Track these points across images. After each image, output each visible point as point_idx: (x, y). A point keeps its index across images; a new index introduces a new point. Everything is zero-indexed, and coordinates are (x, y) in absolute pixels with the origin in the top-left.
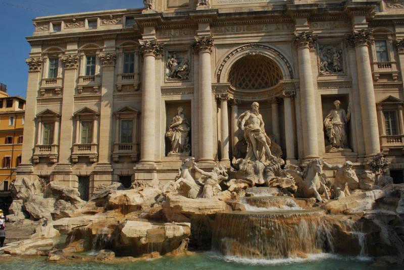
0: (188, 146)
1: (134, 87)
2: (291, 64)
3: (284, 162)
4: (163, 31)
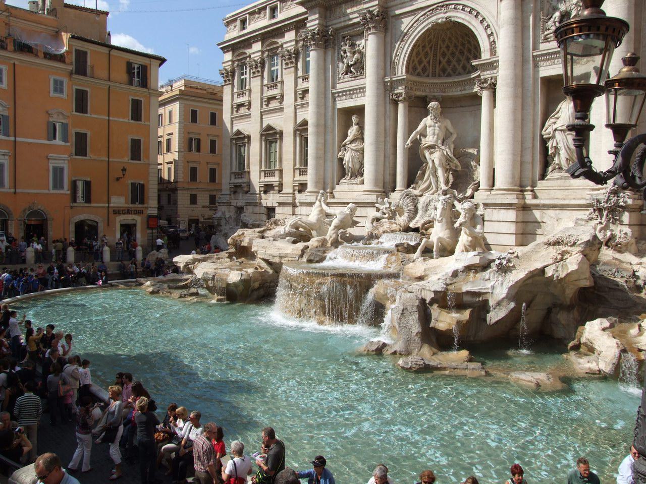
2: (493, 29)
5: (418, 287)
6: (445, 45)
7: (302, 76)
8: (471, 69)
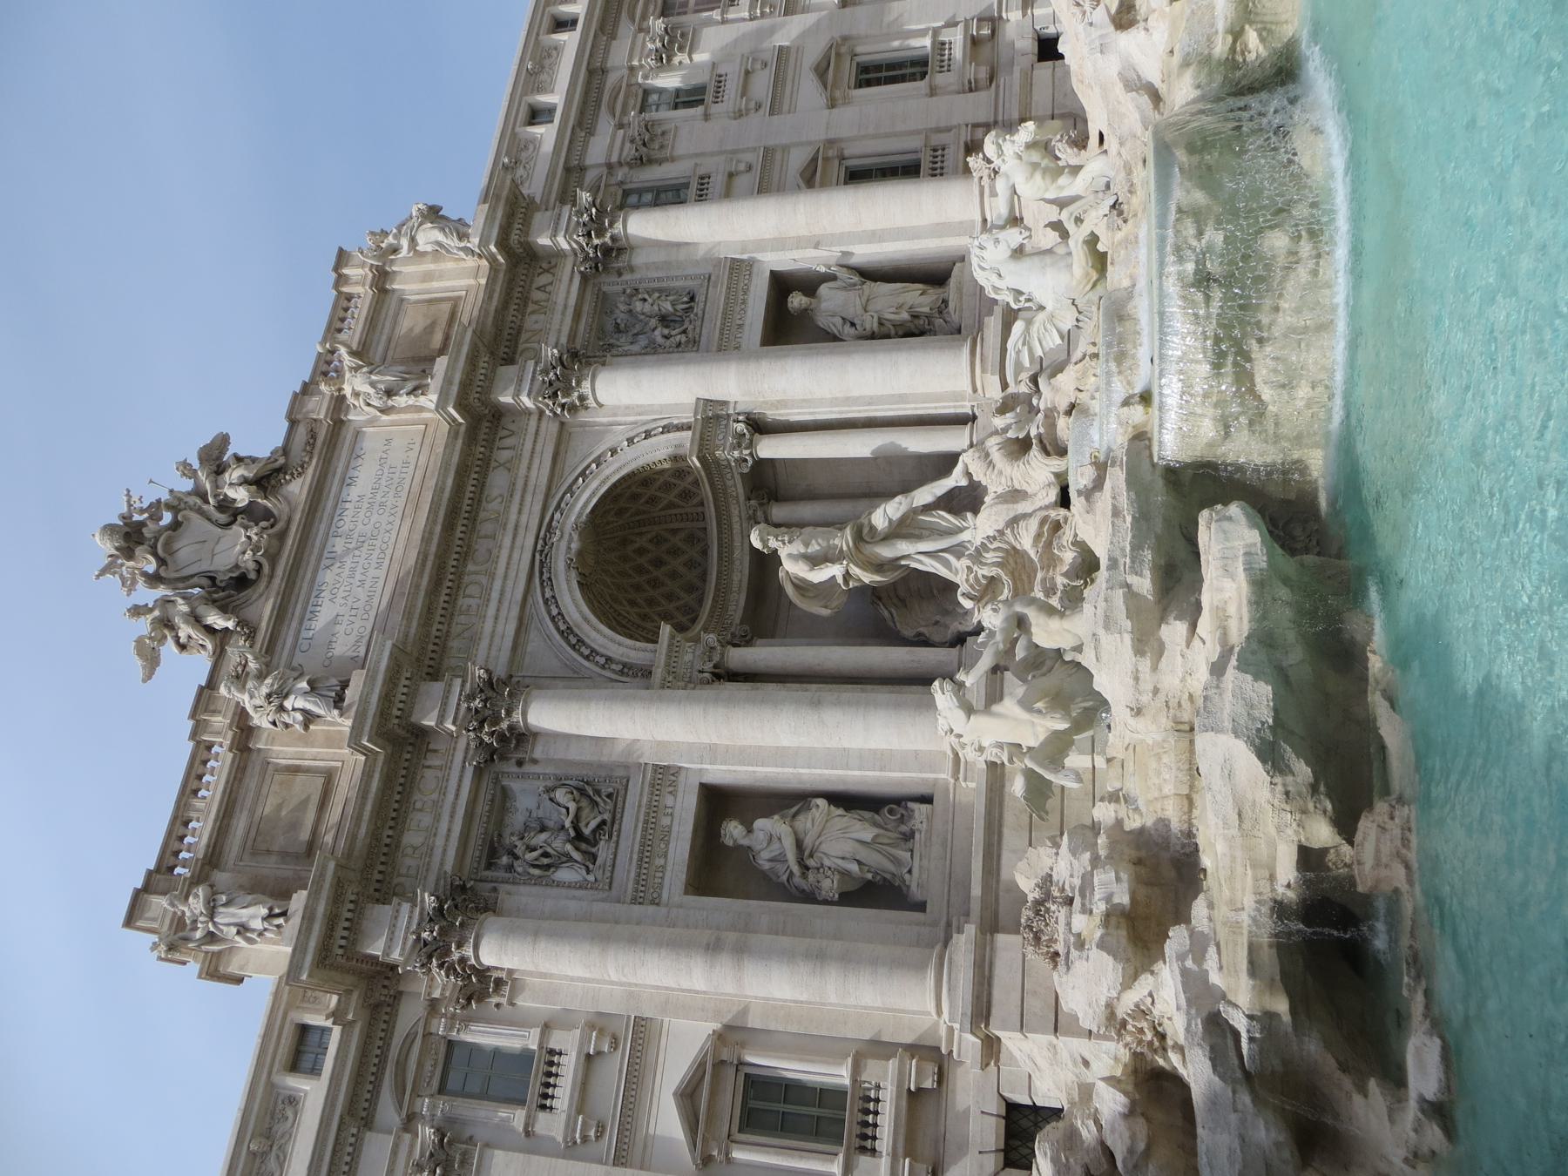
0: (891, 812)
1: (599, 1053)
4: (395, 881)
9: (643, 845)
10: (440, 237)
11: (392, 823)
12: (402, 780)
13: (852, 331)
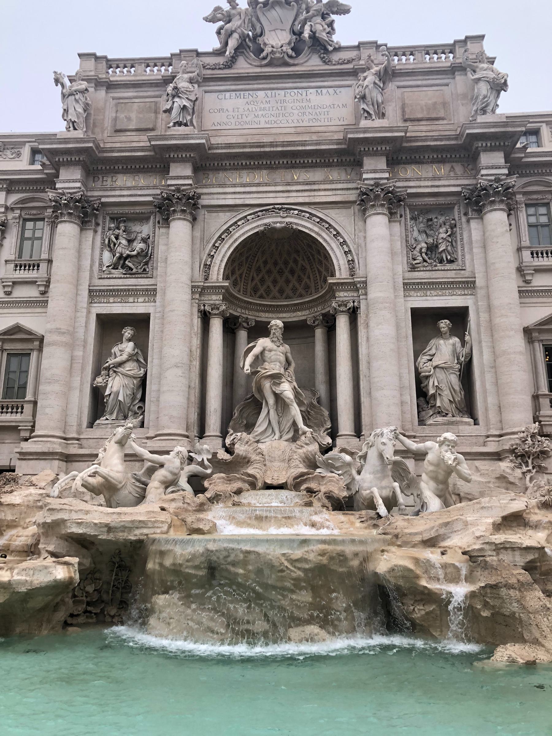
0: (140, 408)
2: (351, 247)
3: (330, 441)
5: (494, 548)
6: (264, 259)
7: (15, 261)
8: (291, 294)
9: (118, 290)
10: (481, 97)
11: (125, 167)
12: (146, 167)
13: (423, 360)
